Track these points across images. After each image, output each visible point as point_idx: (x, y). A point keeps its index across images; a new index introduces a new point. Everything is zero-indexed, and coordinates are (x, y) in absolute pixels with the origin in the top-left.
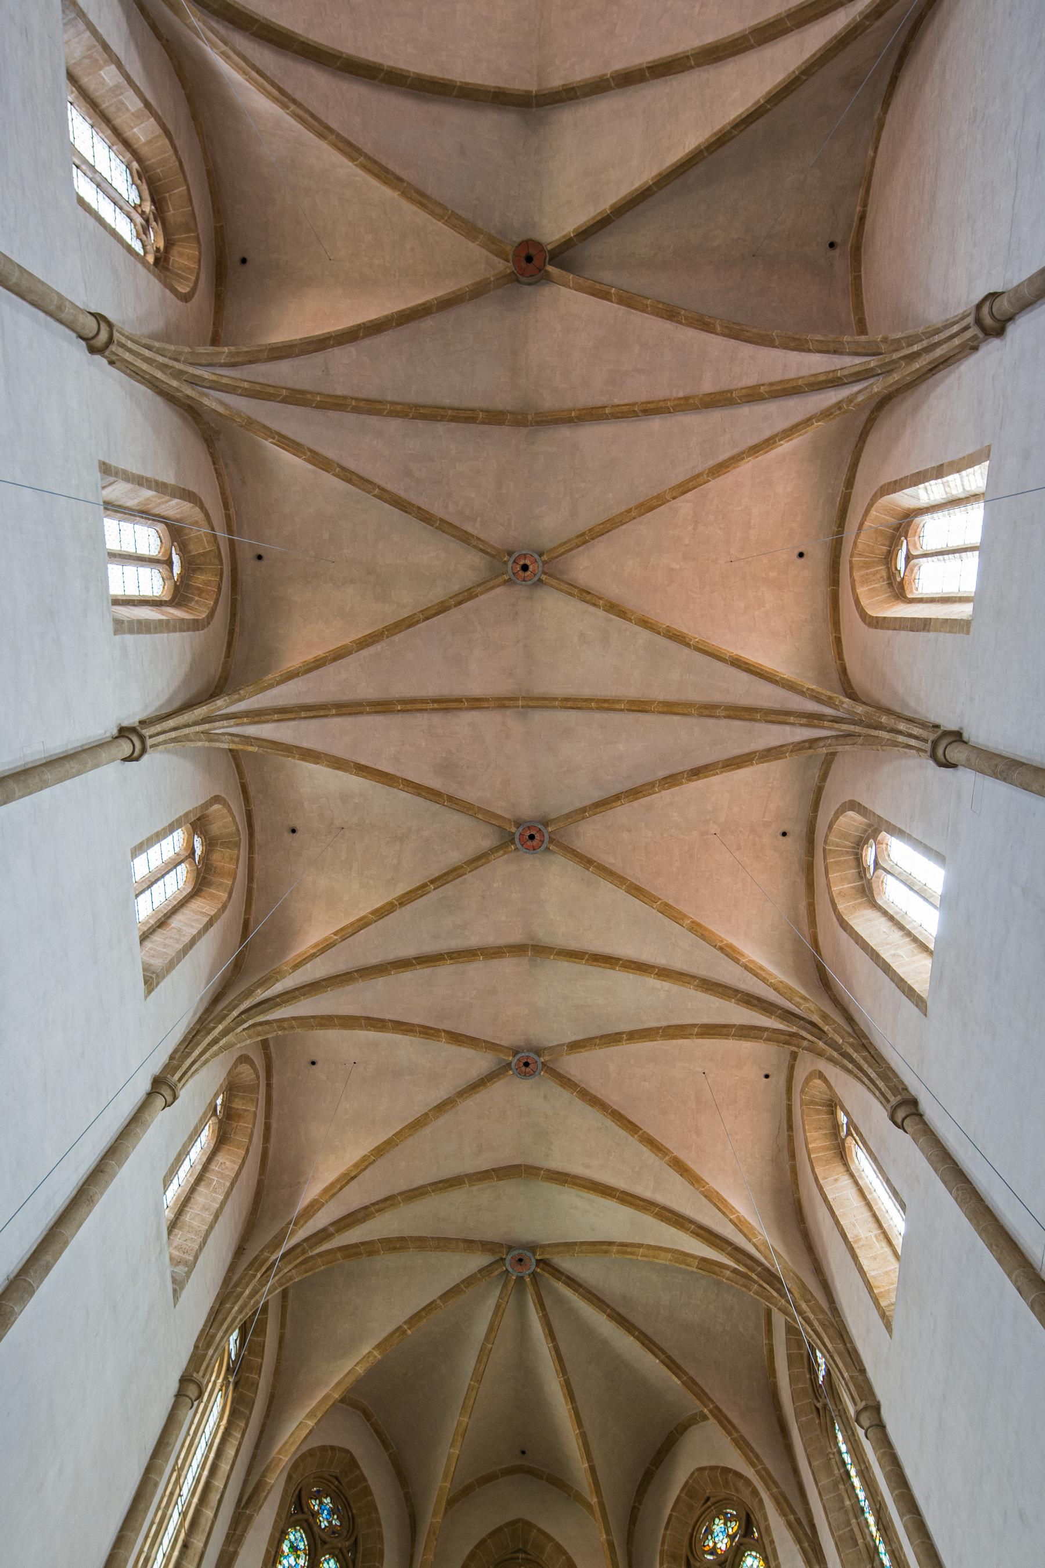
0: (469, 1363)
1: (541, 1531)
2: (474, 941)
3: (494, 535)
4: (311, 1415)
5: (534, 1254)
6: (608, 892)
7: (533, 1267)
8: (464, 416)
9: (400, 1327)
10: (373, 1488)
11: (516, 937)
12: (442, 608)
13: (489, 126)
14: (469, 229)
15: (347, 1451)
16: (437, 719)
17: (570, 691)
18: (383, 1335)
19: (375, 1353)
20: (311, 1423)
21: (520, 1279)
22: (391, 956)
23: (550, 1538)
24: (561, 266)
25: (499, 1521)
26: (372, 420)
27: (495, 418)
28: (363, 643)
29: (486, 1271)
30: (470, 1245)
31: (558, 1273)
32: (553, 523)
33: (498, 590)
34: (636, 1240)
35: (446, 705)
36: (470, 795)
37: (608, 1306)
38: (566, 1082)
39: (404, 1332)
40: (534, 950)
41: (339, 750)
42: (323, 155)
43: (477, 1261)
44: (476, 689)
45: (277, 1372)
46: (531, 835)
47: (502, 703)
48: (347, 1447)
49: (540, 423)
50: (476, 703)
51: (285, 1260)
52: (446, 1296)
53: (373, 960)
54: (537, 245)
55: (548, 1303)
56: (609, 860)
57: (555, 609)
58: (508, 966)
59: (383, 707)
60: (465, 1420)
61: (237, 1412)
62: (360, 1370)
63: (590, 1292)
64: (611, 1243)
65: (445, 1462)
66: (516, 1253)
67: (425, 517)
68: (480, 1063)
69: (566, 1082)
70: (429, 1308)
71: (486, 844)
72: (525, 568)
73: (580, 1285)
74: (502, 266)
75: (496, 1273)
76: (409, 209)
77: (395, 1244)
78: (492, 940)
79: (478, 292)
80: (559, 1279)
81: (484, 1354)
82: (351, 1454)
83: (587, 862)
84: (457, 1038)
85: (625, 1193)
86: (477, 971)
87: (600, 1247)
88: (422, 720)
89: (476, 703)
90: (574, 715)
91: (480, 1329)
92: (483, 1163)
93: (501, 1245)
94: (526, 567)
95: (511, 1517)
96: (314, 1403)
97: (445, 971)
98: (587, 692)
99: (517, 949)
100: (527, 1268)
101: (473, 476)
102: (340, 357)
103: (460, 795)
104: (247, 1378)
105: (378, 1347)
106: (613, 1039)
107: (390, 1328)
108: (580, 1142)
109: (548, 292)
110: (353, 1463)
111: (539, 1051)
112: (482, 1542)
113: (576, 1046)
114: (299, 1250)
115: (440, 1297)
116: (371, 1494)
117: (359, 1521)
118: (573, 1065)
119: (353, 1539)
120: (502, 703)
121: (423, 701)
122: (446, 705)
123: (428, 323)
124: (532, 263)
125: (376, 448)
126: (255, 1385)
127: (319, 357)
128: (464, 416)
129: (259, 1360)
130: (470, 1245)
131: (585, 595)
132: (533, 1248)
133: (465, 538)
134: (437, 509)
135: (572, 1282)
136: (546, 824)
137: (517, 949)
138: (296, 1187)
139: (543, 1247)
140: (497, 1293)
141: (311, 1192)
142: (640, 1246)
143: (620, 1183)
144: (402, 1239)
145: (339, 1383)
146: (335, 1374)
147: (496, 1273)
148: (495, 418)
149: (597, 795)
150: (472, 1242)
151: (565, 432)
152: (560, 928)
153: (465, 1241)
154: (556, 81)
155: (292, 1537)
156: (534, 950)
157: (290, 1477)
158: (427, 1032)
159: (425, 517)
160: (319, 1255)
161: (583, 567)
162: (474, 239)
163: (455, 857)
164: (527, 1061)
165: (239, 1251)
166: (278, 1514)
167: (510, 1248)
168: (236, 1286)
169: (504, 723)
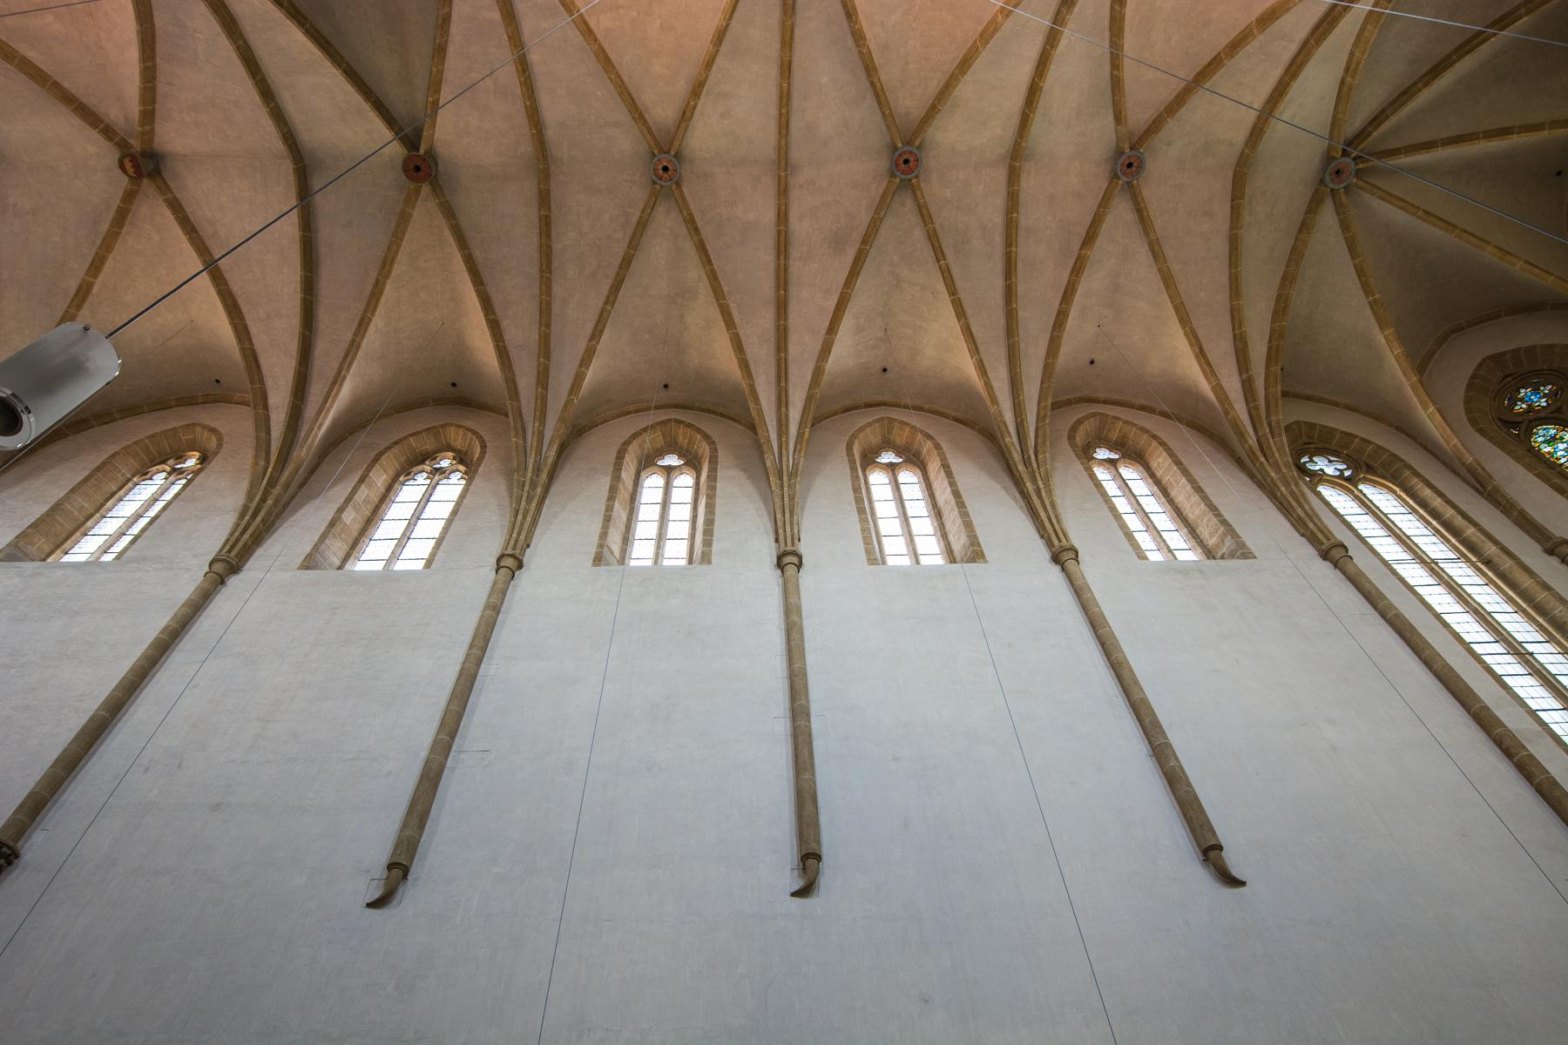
0: (1432, 232)
2: (997, 219)
3: (640, 195)
5: (1334, 158)
6: (965, 89)
7: (1348, 160)
8: (546, 226)
11: (1001, 175)
12: (701, 247)
13: (327, 205)
14: (403, 220)
15: (1484, 360)
16: (795, 252)
17: (772, 127)
18: (1373, 320)
20: (1432, 409)
21: (1359, 173)
22: (1001, 302)
24: (419, 137)
26: (556, 307)
27: (544, 199)
28: (730, 323)
29: (1340, 209)
30: (1305, 227)
31: (1363, 134)
32: (626, 142)
33: (685, 190)
34: (1345, 57)
35: (782, 246)
36: (863, 219)
37: (1415, 83)
38: (1155, 126)
40: (1016, 157)
41: (815, 345)
42: (372, 339)
43: (1328, 217)
44: (768, 216)
46: (905, 161)
47: (783, 192)
49: (545, 157)
50: (782, 217)
52: (1353, 253)
53: (1000, 320)
54: (406, 163)
55: (1396, 145)
56: (934, 85)
57: (703, 138)
58: (1029, 184)
59: (782, 307)
62: (1398, 351)
63: (1394, 102)
64: (1343, 81)
66: (1327, 179)
67: (627, 262)
68: (1121, 209)
69: (1155, 126)
70: (1360, 272)
71: (910, 204)
72: (665, 169)
73: (1383, 111)
74: (426, 189)
75: (1344, 198)
76: (397, 269)
77: (1281, 306)
78: (1000, 201)
79: (449, 213)
80: (1370, 134)
83: (933, 110)
84: (1089, 239)
85: (1287, 70)
86: (1029, 216)
87: (1344, 92)
88: (795, 266)
89: (782, 217)
90: (794, 124)
91: (1400, 217)
92: (1222, 210)
93: (1316, 191)
94: (666, 165)
96: (1415, 399)
97: (1024, 249)
98: (773, 112)
99: (1013, 176)
100: (1350, 162)
101: (594, 213)
102: (512, 333)
103: (862, 230)
104: (1370, 456)
105: (1382, 328)
106: (1116, 84)
107: (1369, 312)
108: (1222, 117)
109: (441, 150)
110: (1497, 358)
111: (1119, 152)
113: (1119, 118)
115: (1353, 258)
116: (1535, 347)
118: (1138, 116)
120: (783, 192)
121: (778, 266)
122: (782, 246)
123: (478, 255)
124: (421, 166)
125: (577, 306)
127: (513, 353)
128: (546, 226)
130: (1305, 227)
131: (686, 115)
132: (1328, 158)
133: (642, 226)
134: (620, 249)
135: (1377, 119)
136: (895, 148)
137: (1013, 176)
138: (1199, 397)
139: (1330, 149)
140: (1369, 196)
141: (1205, 387)
142: (1352, 54)
143: (1276, 74)
144: (1278, 298)
146: (1393, 368)
147: (1344, 198)
148: (544, 199)
149: (870, 100)
150: (1303, 223)
151: (551, 134)
152: (997, 131)
153: (1300, 231)
154: (279, 145)
156: (1016, 157)
158: (1078, 269)
159: (627, 262)
160: (1266, 389)
161: (663, 112)
162: (410, 215)
163: (918, 234)
164: (1127, 165)
165: (1239, 462)
166: (1509, 453)
167: (1322, 182)
169: (801, 186)
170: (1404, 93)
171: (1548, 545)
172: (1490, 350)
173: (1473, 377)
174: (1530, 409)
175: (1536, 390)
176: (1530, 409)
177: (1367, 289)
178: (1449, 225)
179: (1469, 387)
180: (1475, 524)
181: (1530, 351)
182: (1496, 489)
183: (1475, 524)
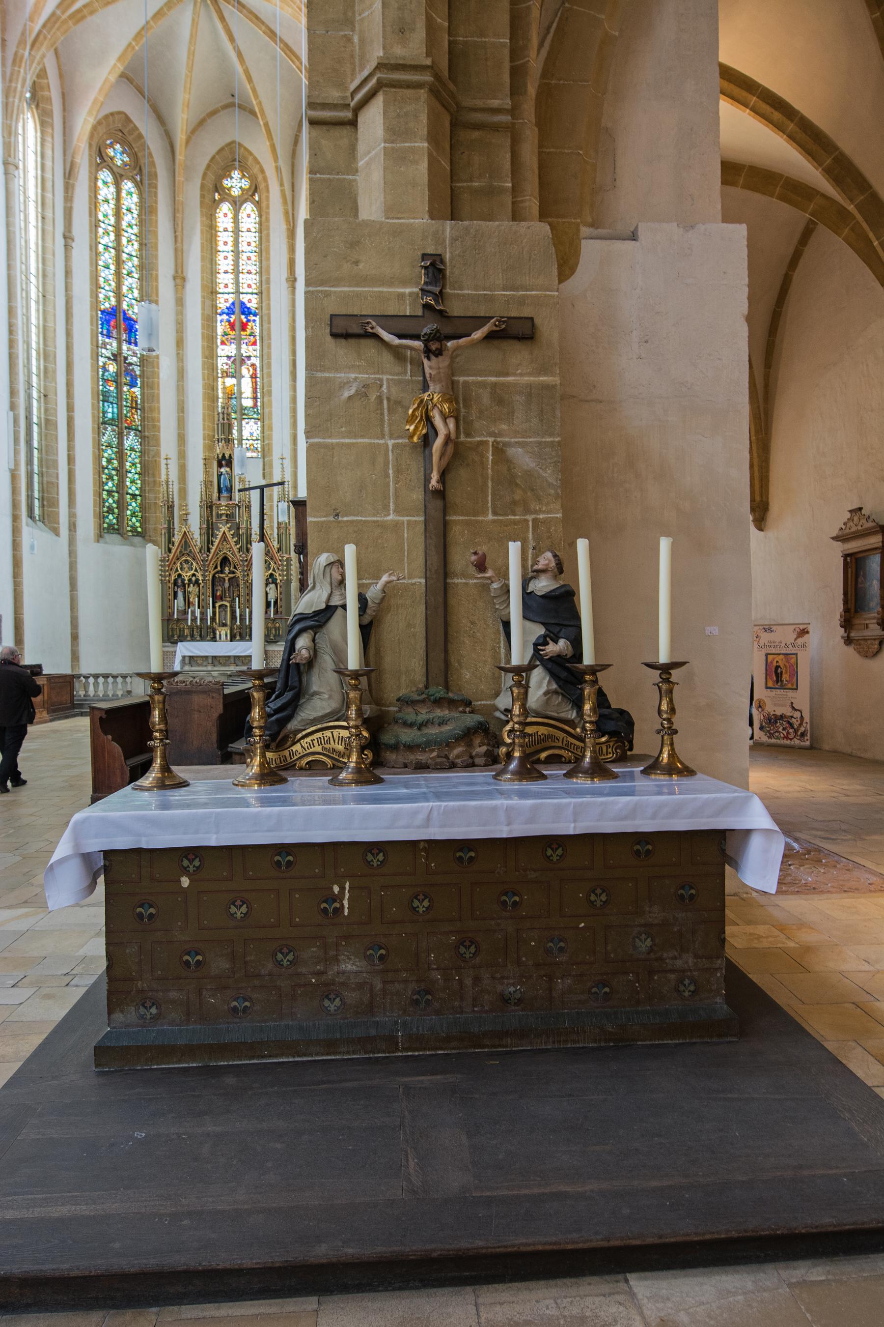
1: (246, 149)
4: (90, 113)
9: (130, 44)
10: (144, 133)
19: (119, 65)
23: (251, 153)
25: (222, 143)
37: (263, 23)
39: (133, 48)
45: (61, 76)
48: (122, 110)
51: (35, 48)
60: (187, 96)
61: (44, 123)
65: (182, 120)
81: (191, 54)
82: (125, 114)
95: (228, 140)
104: (43, 96)
107: (125, 44)
110: (128, 120)
112: (213, 158)
114: (41, 37)
117: (139, 155)
119: (138, 168)
126: (49, 100)
129: (46, 81)
145: (101, 89)
155: (102, 177)
157: (90, 145)
168: (11, 81)
170: (257, 18)
171: (67, 234)
172: (129, 111)
173: (112, 114)
174: (112, 159)
175: (123, 153)
176: (112, 159)
177: (138, 36)
178: (190, 69)
179: (106, 117)
180: (53, 195)
181: (140, 136)
182: (73, 186)
183: (53, 195)
